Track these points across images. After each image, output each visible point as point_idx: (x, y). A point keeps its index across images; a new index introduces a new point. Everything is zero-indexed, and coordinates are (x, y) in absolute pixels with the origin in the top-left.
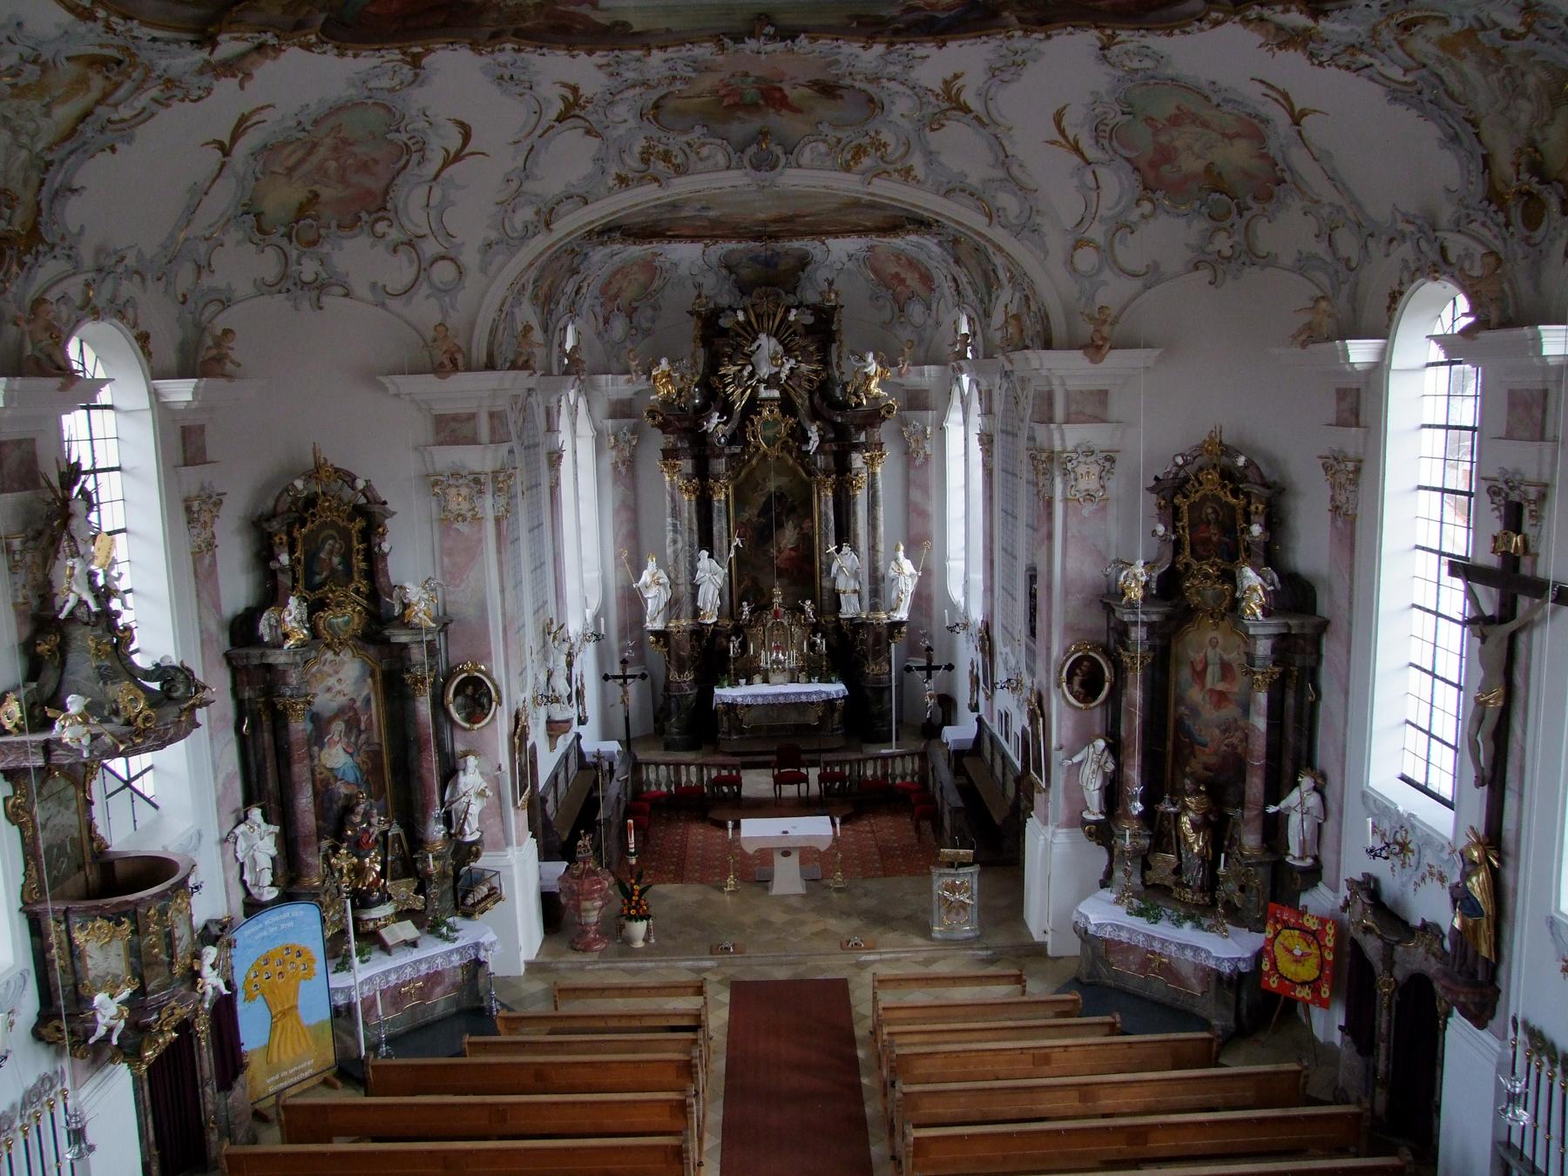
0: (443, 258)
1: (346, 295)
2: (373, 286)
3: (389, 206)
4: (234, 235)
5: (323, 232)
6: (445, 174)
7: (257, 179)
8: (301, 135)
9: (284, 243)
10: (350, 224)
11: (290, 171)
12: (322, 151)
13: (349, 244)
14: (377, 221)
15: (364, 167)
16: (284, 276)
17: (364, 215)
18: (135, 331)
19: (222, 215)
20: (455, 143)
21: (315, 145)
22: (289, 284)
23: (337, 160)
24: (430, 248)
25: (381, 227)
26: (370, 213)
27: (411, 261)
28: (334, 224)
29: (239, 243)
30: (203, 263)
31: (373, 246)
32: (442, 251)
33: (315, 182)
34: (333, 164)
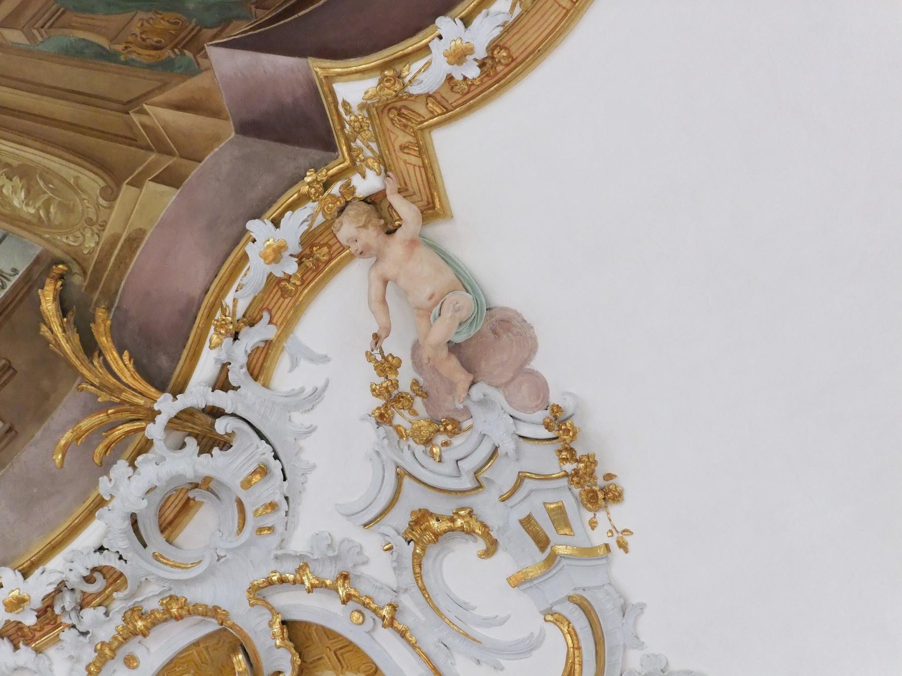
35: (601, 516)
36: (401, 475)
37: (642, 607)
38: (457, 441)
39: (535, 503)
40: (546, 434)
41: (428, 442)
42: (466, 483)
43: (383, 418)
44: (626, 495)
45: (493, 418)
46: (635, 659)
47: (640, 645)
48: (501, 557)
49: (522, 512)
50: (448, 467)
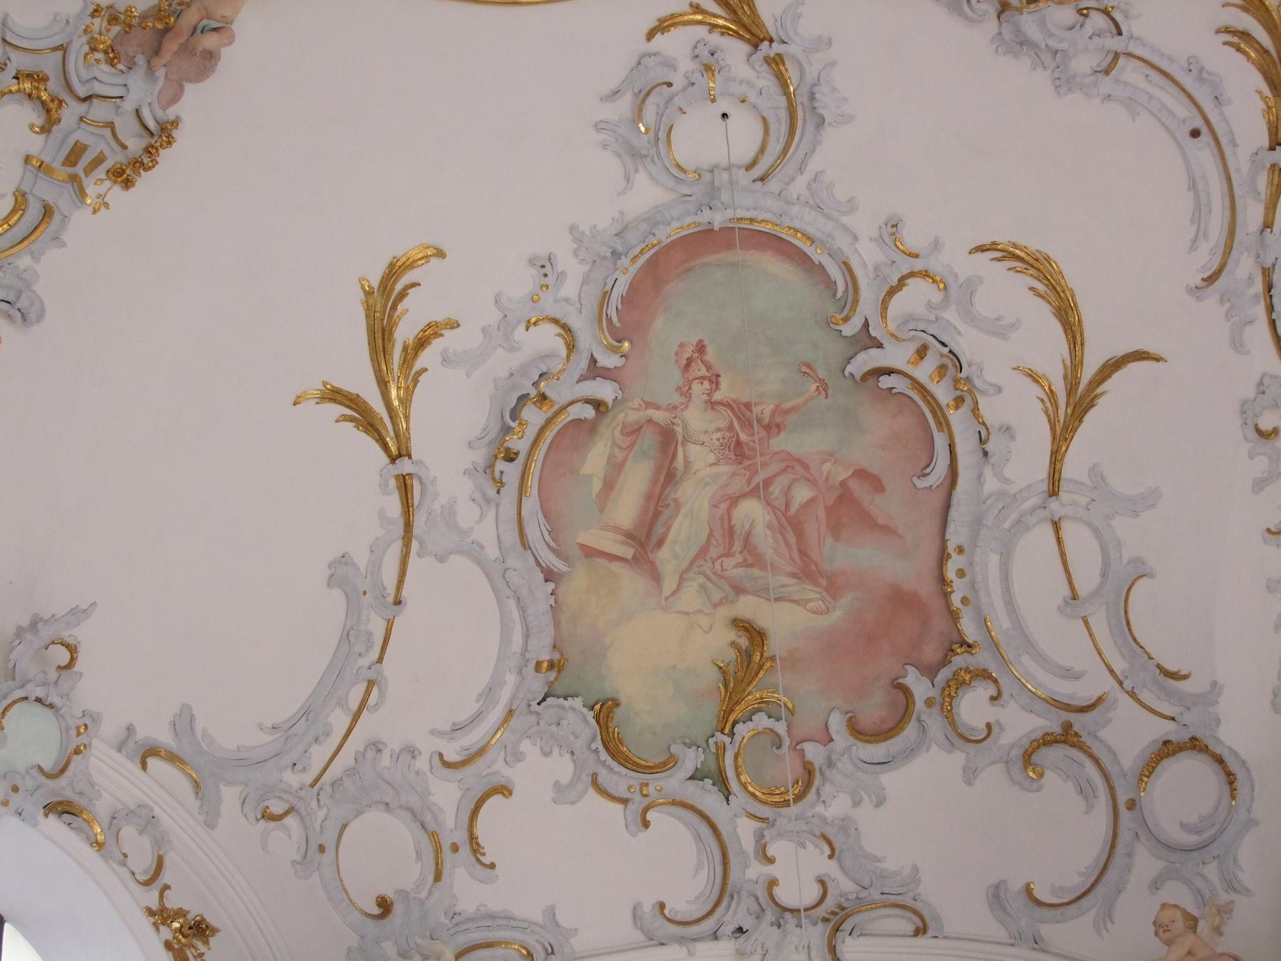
0: (1167, 749)
1: (920, 931)
2: (997, 896)
3: (970, 631)
4: (540, 770)
5: (813, 752)
6: (1073, 467)
7: (549, 575)
8: (605, 391)
9: (709, 799)
10: (886, 726)
11: (644, 540)
12: (702, 463)
13: (890, 780)
14: (959, 683)
15: (848, 508)
16: (724, 892)
17: (920, 687)
18: (151, 898)
19: (488, 695)
20: (1044, 345)
21: (668, 439)
22: (738, 914)
23: (759, 491)
24: (1128, 733)
25: (974, 706)
26: (930, 672)
27: (1085, 791)
28: (837, 723)
29: (562, 792)
30: (451, 829)
31: (970, 775)
32: (1165, 729)
33: (739, 590)
34: (752, 513)
35: (108, 184)
36: (63, 48)
37: (64, 245)
38: (105, 67)
39: (97, 143)
40: (151, 124)
41: (93, 50)
42: (82, 91)
43: (96, 12)
44: (132, 190)
45: (141, 90)
46: (24, 262)
47: (36, 259)
48: (40, 139)
49: (81, 136)
50: (85, 75)
